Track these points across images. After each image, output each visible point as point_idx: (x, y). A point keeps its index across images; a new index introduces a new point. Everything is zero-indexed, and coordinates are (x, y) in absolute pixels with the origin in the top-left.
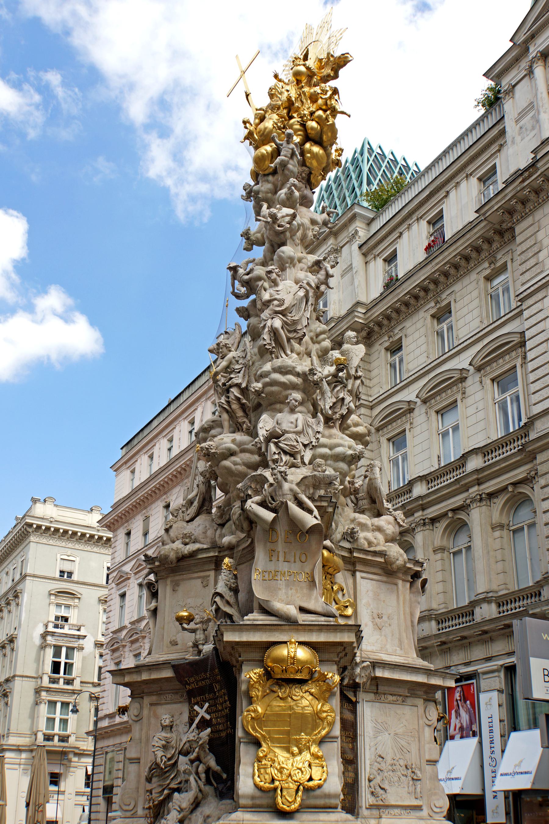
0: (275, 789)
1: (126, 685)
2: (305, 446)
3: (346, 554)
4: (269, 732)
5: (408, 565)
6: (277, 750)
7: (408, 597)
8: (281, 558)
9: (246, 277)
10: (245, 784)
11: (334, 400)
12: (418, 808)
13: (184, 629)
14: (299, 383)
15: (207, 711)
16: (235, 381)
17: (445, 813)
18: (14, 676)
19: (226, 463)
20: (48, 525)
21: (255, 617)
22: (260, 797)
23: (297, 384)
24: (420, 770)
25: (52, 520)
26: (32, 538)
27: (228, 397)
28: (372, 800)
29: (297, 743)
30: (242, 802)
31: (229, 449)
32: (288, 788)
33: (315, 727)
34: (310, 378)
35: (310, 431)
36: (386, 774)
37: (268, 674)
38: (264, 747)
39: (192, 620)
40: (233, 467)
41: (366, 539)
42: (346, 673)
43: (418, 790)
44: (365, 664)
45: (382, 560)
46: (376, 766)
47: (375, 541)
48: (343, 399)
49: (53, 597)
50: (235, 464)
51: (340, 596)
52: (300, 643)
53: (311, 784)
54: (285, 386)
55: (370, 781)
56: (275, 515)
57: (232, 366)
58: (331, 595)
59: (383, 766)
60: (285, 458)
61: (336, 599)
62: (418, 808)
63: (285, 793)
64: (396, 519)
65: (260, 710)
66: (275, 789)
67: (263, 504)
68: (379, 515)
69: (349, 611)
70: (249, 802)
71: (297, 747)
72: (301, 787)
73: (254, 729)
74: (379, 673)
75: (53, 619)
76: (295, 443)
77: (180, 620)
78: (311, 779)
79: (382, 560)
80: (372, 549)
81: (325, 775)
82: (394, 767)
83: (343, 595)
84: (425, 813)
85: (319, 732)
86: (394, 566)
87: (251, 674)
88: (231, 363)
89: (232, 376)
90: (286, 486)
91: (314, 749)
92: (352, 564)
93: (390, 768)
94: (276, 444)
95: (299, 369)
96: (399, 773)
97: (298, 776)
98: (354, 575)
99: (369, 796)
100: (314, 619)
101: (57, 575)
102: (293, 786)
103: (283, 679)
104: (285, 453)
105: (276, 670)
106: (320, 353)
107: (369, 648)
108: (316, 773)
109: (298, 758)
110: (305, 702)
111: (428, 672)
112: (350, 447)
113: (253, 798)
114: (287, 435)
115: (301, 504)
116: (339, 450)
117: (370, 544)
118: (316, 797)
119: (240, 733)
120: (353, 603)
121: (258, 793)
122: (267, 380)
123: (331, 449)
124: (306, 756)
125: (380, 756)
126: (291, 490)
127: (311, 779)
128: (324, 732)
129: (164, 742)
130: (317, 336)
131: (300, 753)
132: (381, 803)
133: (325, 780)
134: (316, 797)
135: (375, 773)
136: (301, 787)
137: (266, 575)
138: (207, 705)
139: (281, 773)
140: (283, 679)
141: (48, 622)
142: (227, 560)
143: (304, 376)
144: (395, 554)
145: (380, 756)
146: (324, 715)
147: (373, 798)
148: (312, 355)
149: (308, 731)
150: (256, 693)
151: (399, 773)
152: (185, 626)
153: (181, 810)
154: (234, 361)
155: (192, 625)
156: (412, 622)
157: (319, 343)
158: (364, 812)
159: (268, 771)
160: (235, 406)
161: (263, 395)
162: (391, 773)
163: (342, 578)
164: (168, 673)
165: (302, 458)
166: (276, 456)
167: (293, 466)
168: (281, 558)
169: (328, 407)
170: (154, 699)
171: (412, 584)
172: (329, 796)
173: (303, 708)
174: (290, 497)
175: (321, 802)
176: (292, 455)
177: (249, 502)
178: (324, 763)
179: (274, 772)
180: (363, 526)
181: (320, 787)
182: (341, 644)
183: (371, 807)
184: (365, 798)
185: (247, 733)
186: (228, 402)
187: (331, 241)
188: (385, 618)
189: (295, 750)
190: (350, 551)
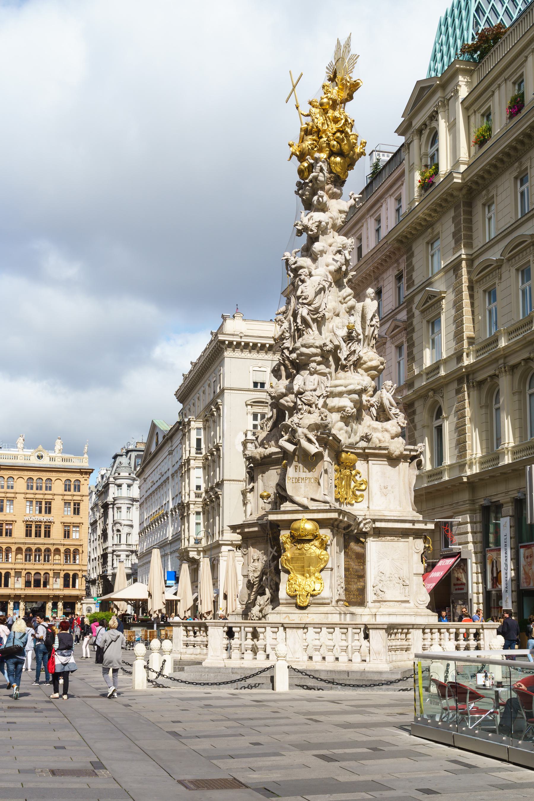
0: (296, 595)
1: (238, 533)
2: (319, 397)
3: (361, 451)
4: (294, 566)
5: (405, 453)
6: (298, 575)
7: (407, 472)
8: (301, 470)
9: (293, 266)
10: (283, 594)
11: (348, 353)
12: (407, 602)
13: (265, 502)
14: (318, 352)
15: (276, 551)
16: (286, 345)
17: (427, 605)
18: (223, 481)
19: (282, 401)
20: (239, 340)
21: (287, 506)
22: (289, 599)
23: (317, 354)
24: (409, 579)
25: (241, 335)
26: (226, 354)
27: (283, 356)
28: (375, 598)
29: (309, 572)
30: (281, 601)
31: (282, 393)
32: (302, 595)
33: (318, 562)
34: (325, 348)
35: (322, 385)
36: (385, 583)
37: (292, 536)
38: (292, 575)
39: (269, 497)
40: (286, 404)
41: (377, 438)
42: (352, 528)
43: (407, 591)
44: (368, 521)
45: (386, 452)
46: (379, 578)
47: (383, 439)
48: (355, 351)
49: (249, 407)
50: (287, 402)
51: (357, 478)
52: (308, 519)
53: (314, 593)
54: (309, 356)
55: (374, 587)
56: (294, 447)
57: (285, 334)
58: (350, 478)
59: (383, 578)
60: (305, 407)
61: (354, 480)
62: (407, 602)
63: (301, 597)
64: (398, 423)
65: (289, 555)
66: (296, 595)
67: (289, 441)
68: (388, 419)
69: (363, 487)
70: (284, 602)
71: (308, 573)
72: (309, 594)
73: (286, 564)
74: (378, 525)
75: (251, 428)
76: (310, 398)
77: (262, 497)
78: (314, 590)
79: (386, 452)
80: (380, 445)
81: (322, 588)
82: (391, 579)
83: (360, 477)
84: (411, 605)
85: (320, 566)
86: (394, 455)
87: (284, 535)
88: (284, 332)
89: (284, 341)
90: (300, 430)
91: (317, 574)
92: (365, 457)
93: (388, 579)
94: (300, 399)
95: (317, 344)
96: (394, 582)
97: (308, 589)
98: (368, 463)
99: (373, 595)
100: (318, 505)
101: (251, 386)
102: (305, 594)
103: (299, 539)
104: (305, 404)
105: (296, 535)
106: (348, 310)
107: (377, 508)
108: (318, 587)
109: (308, 579)
110: (312, 551)
111: (413, 522)
112: (358, 384)
113: (286, 600)
114: (307, 393)
115: (310, 441)
116: (350, 388)
117: (380, 441)
118: (318, 599)
119: (280, 568)
120: (366, 482)
121: (289, 597)
122: (298, 352)
123: (345, 387)
124: (313, 578)
125: (381, 572)
126: (303, 433)
127: (314, 590)
128: (322, 566)
129: (254, 569)
130: (344, 299)
131: (310, 576)
132: (381, 599)
133: (322, 590)
134: (318, 599)
135: (378, 583)
136: (309, 594)
137: (294, 479)
138: (276, 548)
139: (299, 587)
140: (299, 539)
141: (247, 431)
142: (284, 462)
143: (321, 347)
144: (394, 448)
145: (381, 572)
146: (322, 557)
147: (376, 597)
148: (341, 314)
149: (314, 565)
150: (288, 546)
151: (394, 582)
152: (265, 501)
153: (260, 606)
154: (285, 330)
155: (270, 500)
156: (410, 488)
157: (346, 303)
158: (370, 604)
159: (293, 586)
160: (287, 362)
161: (297, 361)
162: (389, 582)
163: (360, 465)
164: (256, 529)
165: (316, 405)
166: (300, 407)
167: (310, 412)
168: (301, 470)
169: (343, 359)
170: (253, 541)
171: (410, 463)
172: (325, 599)
173: (311, 553)
174: (303, 436)
175: (321, 601)
176: (310, 405)
177: (281, 441)
178: (322, 582)
179: (297, 588)
180: (375, 429)
181: (319, 594)
182: (331, 519)
183: (375, 601)
184: (370, 596)
185: (282, 567)
186: (283, 360)
187: (439, 94)
188: (389, 488)
189: (308, 575)
190: (364, 449)
